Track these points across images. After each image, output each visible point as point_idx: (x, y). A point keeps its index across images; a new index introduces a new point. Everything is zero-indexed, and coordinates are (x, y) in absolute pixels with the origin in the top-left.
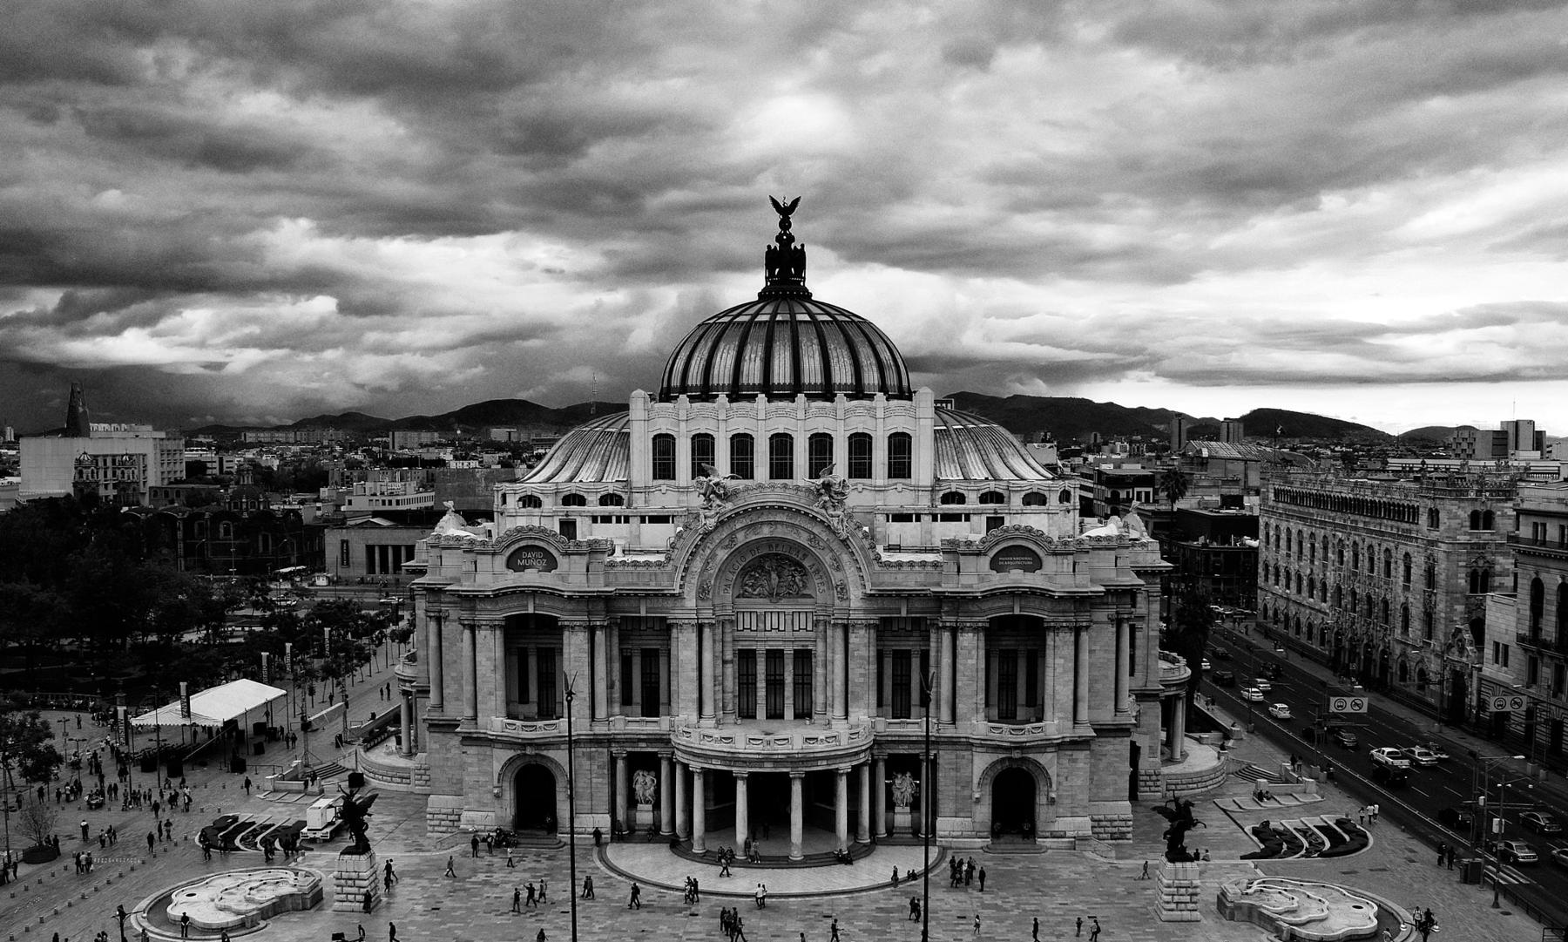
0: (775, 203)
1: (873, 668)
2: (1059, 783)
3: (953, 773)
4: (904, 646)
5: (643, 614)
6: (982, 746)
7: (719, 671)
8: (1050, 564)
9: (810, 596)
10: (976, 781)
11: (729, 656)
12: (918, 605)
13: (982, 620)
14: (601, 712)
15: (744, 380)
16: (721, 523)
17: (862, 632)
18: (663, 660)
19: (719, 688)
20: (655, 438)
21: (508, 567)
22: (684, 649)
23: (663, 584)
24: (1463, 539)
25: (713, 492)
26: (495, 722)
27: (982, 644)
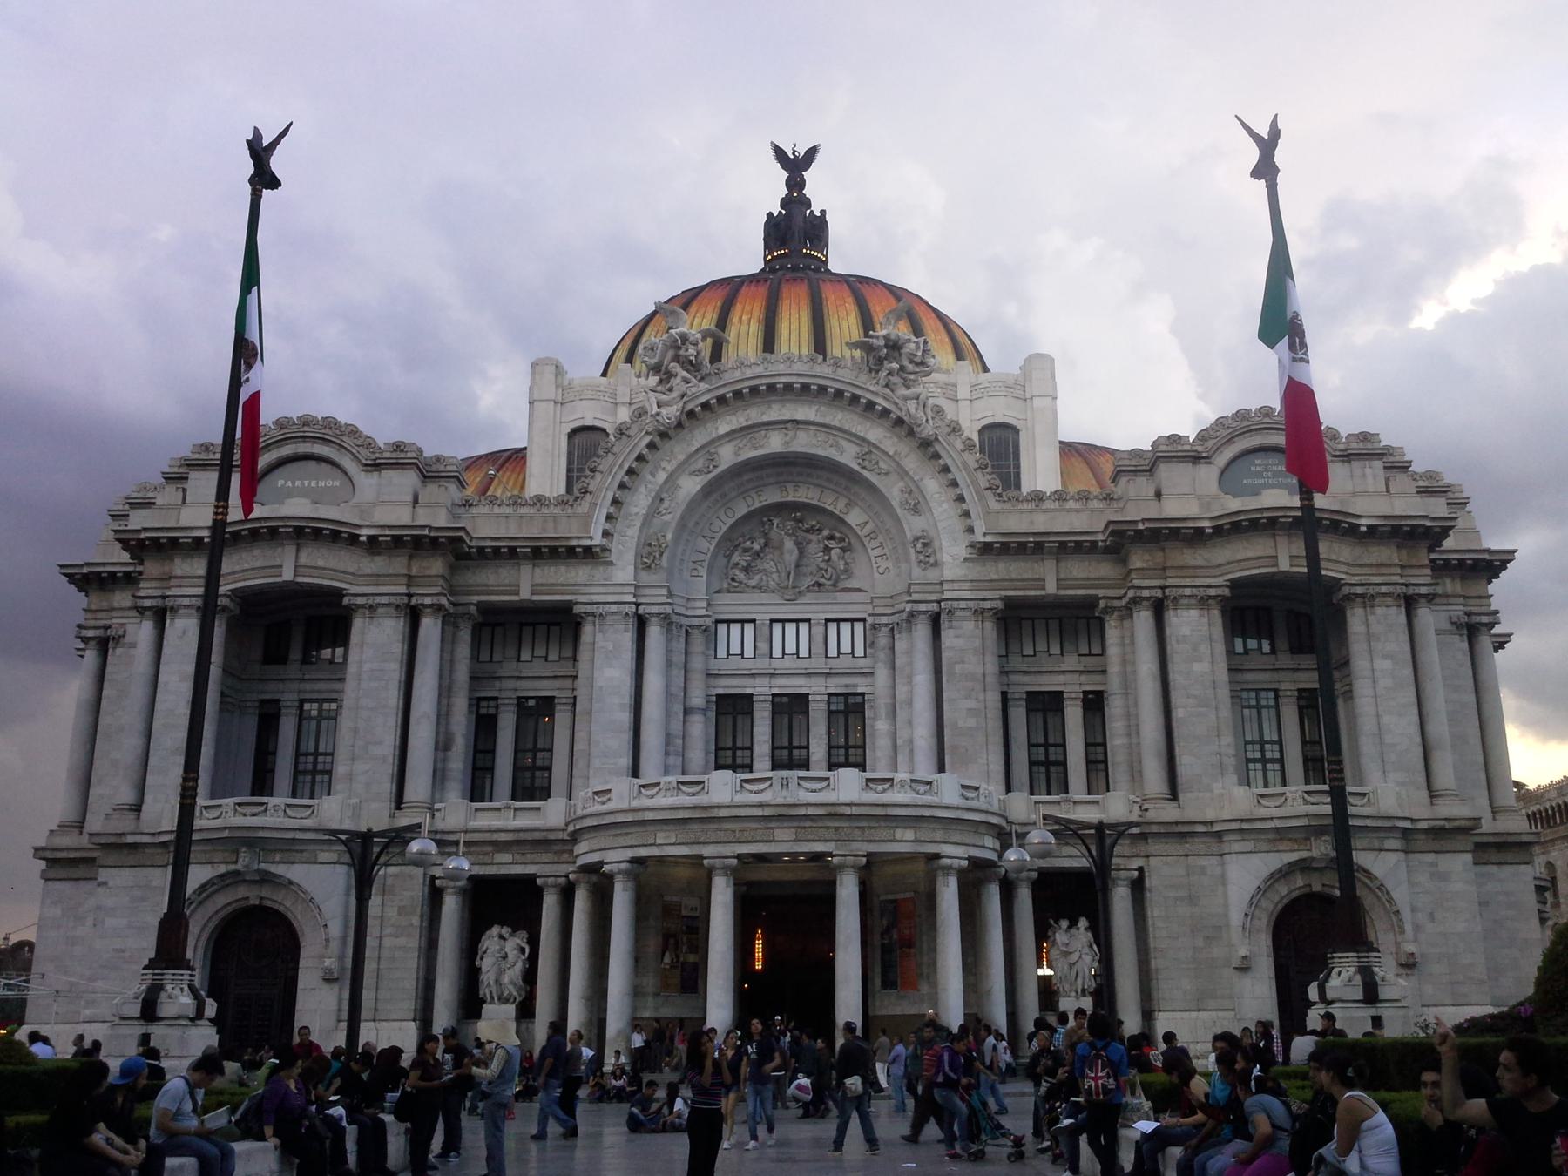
0: (780, 154)
1: (994, 698)
2: (1417, 928)
5: (525, 594)
7: (676, 727)
8: (1338, 474)
9: (859, 590)
10: (1236, 918)
11: (697, 700)
12: (1078, 569)
13: (1218, 582)
17: (969, 626)
18: (561, 718)
19: (674, 761)
20: (574, 433)
23: (566, 528)
25: (676, 359)
27: (1218, 631)
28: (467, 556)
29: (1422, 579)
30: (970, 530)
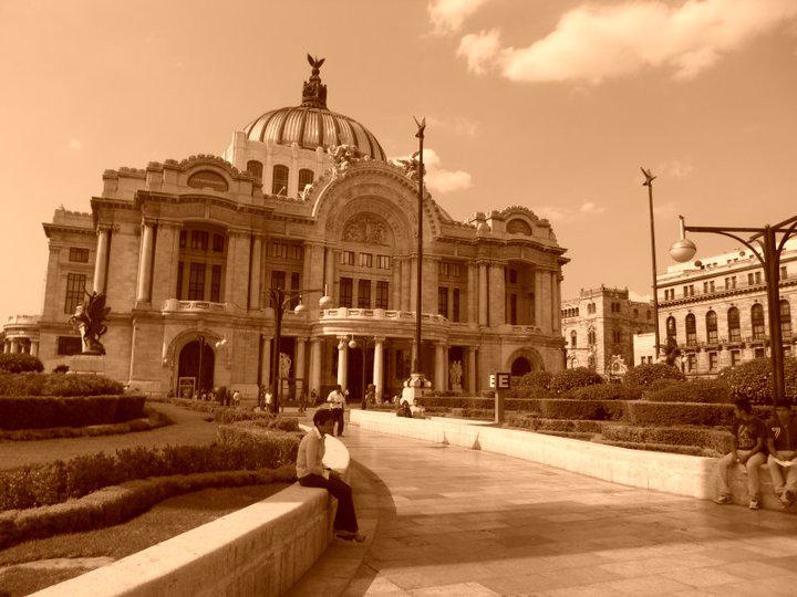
0: (310, 59)
3: (489, 360)
4: (445, 285)
6: (508, 339)
11: (338, 280)
12: (465, 249)
13: (505, 260)
14: (255, 302)
15: (306, 139)
16: (347, 177)
20: (248, 163)
21: (190, 183)
22: (314, 267)
23: (303, 213)
24: (609, 316)
26: (168, 305)
28: (269, 218)
29: (555, 265)
30: (434, 233)
